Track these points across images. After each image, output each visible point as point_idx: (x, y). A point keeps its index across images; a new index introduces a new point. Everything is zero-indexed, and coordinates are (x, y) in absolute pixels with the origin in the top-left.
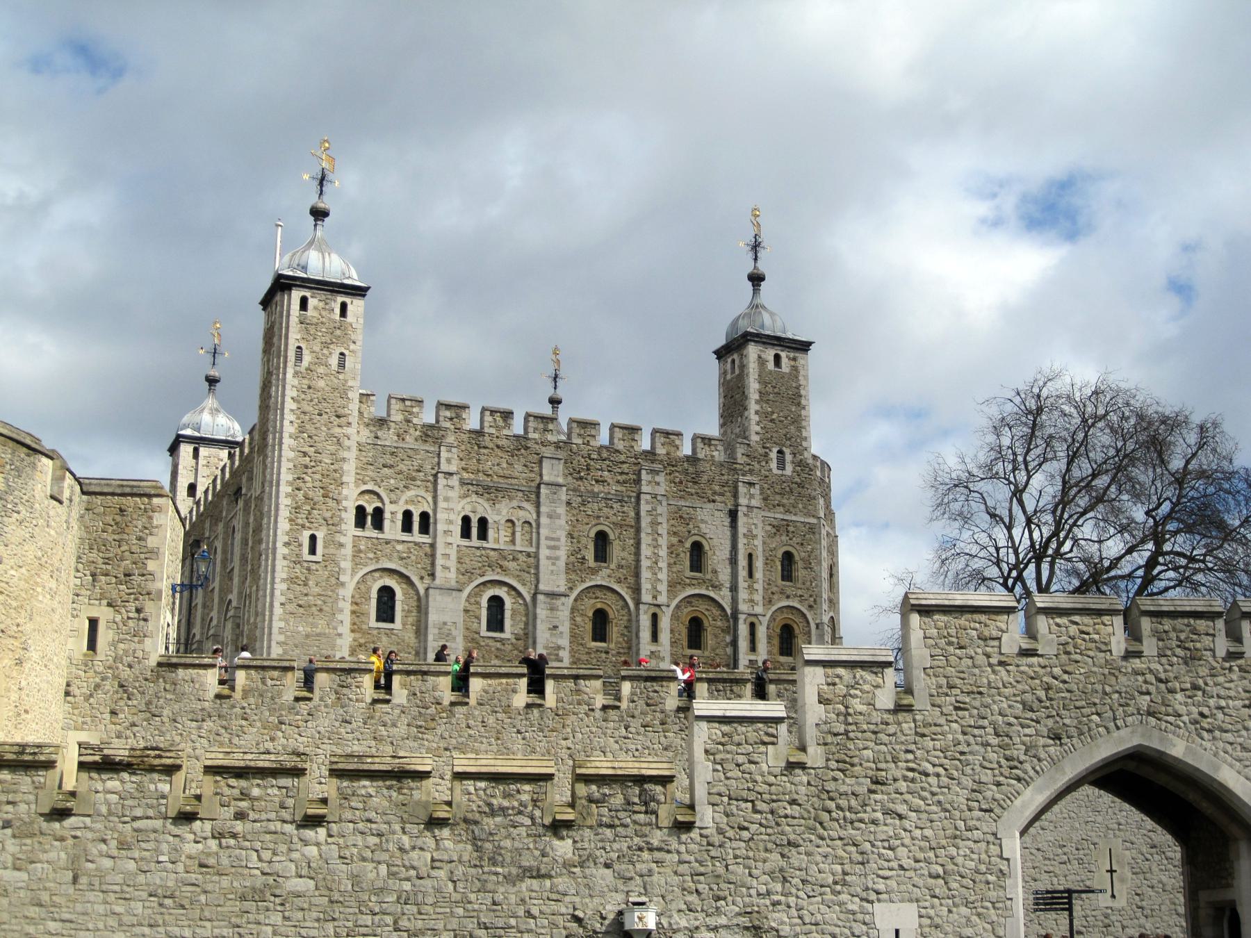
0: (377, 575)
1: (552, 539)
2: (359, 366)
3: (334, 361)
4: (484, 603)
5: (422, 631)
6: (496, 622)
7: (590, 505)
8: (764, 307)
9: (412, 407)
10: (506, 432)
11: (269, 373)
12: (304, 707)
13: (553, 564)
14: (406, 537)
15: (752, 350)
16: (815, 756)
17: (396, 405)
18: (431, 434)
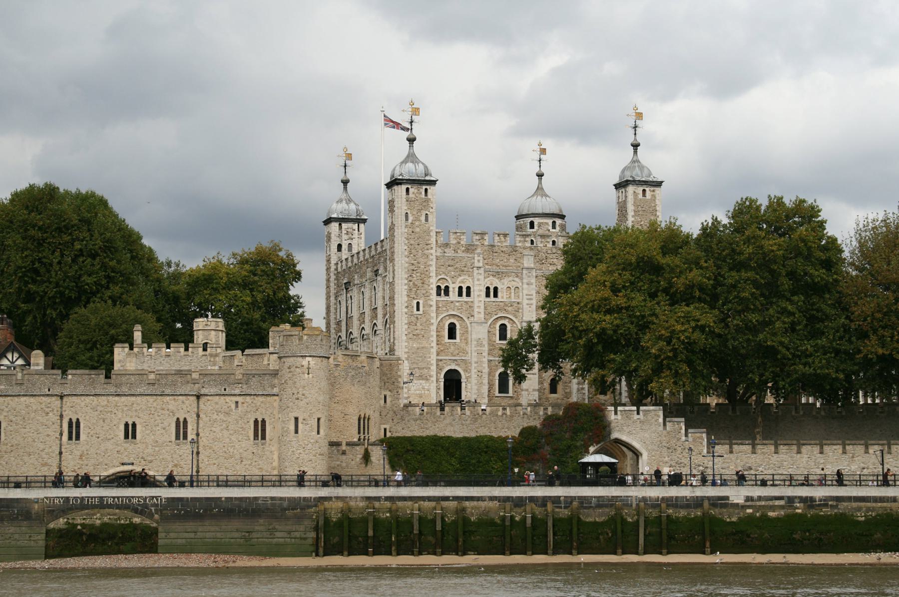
0: (447, 318)
1: (530, 295)
2: (435, 220)
3: (423, 218)
4: (498, 328)
5: (470, 343)
6: (503, 336)
8: (638, 161)
9: (460, 236)
10: (505, 244)
11: (392, 222)
12: (442, 416)
13: (530, 307)
14: (460, 299)
15: (631, 189)
17: (452, 236)
18: (470, 248)
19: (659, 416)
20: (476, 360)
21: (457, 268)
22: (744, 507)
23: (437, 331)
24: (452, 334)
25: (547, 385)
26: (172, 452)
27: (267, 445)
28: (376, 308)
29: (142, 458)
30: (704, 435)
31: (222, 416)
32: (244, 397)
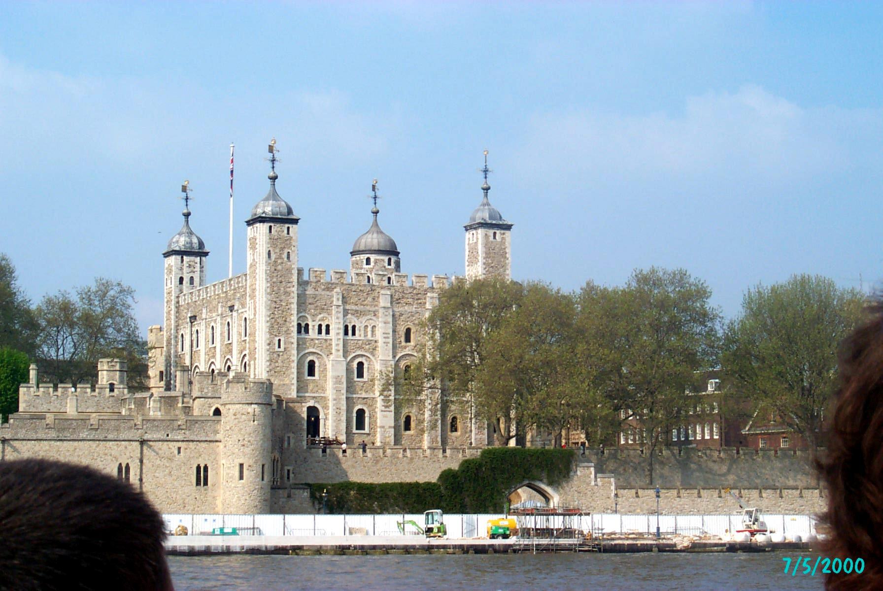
0: (307, 355)
1: (387, 334)
3: (285, 256)
7: (404, 316)
8: (488, 204)
11: (254, 260)
13: (387, 345)
15: (481, 232)
18: (329, 287)
20: (335, 397)
21: (317, 307)
23: (297, 369)
24: (311, 372)
27: (210, 490)
28: (230, 344)
30: (612, 480)
31: (165, 462)
32: (187, 443)
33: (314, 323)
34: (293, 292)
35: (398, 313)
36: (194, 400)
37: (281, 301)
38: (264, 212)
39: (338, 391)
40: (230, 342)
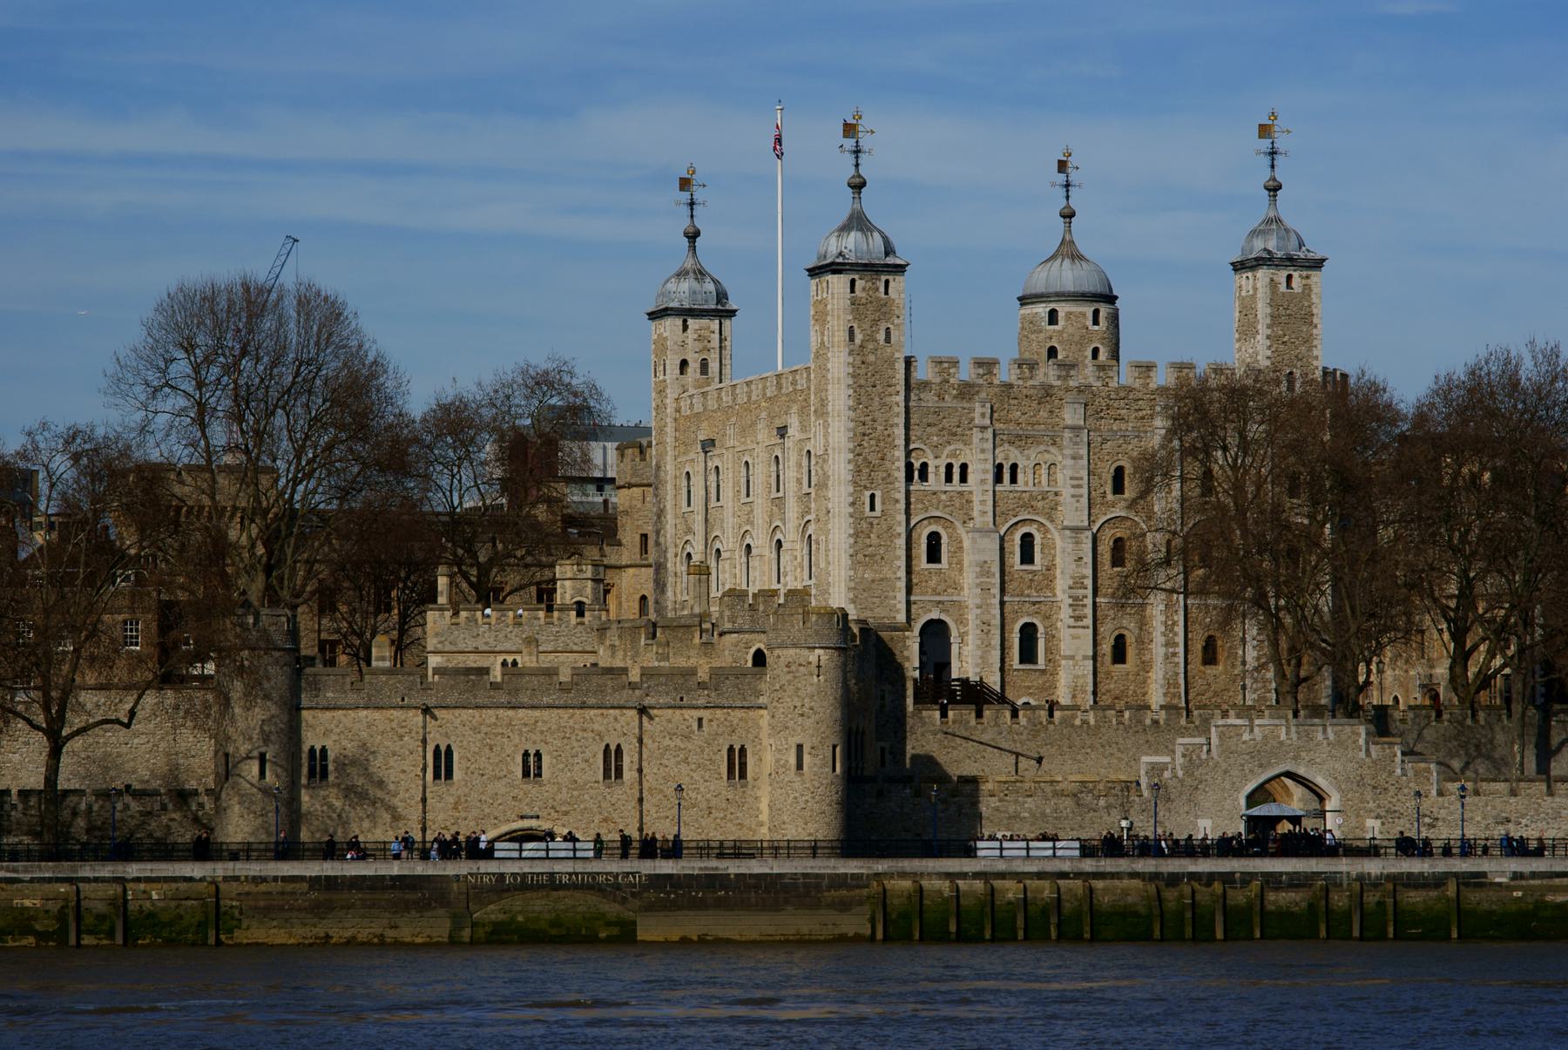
0: (925, 522)
1: (1077, 479)
3: (881, 336)
6: (1027, 557)
8: (1278, 220)
11: (823, 343)
14: (948, 488)
15: (1263, 274)
16: (1180, 773)
18: (967, 391)
19: (1359, 734)
21: (943, 429)
22: (1509, 888)
24: (934, 555)
25: (1106, 647)
26: (600, 798)
29: (553, 807)
31: (678, 742)
33: (937, 462)
34: (897, 404)
35: (1099, 439)
36: (721, 635)
37: (874, 421)
38: (840, 254)
39: (985, 590)
40: (781, 494)
